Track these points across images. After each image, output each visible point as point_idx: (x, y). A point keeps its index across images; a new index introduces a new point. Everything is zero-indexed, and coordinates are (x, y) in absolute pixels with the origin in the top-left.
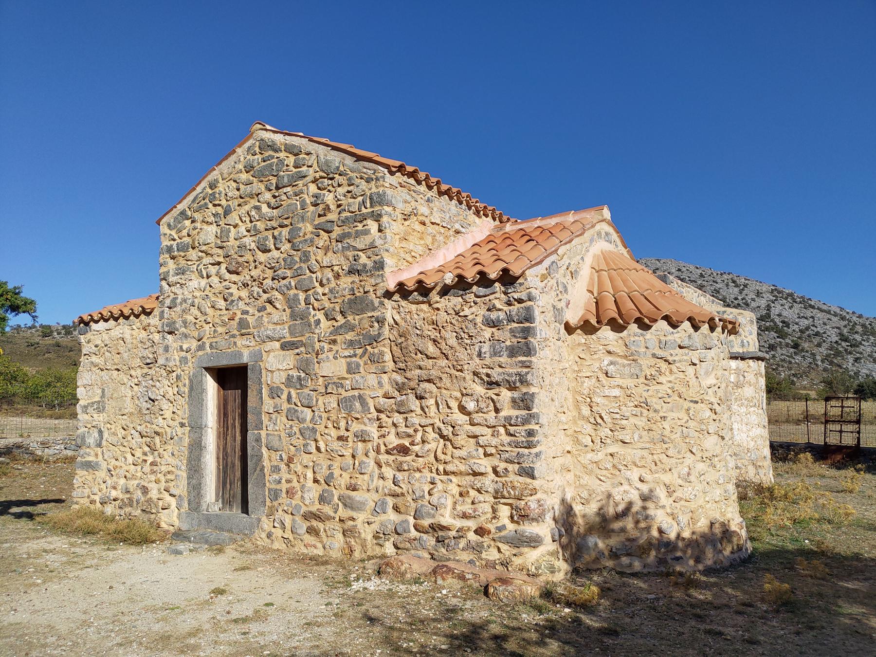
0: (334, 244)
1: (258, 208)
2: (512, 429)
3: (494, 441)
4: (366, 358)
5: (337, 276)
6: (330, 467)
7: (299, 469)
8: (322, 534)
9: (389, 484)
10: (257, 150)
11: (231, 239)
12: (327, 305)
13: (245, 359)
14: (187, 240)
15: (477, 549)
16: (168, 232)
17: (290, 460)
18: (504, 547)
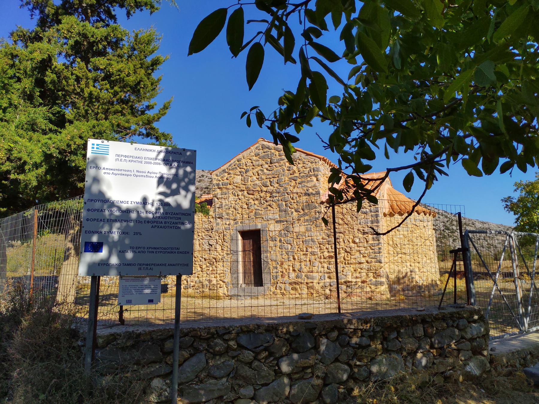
0: (298, 184)
1: (262, 171)
2: (373, 248)
3: (366, 252)
4: (314, 225)
5: (300, 196)
6: (300, 265)
7: (286, 267)
8: (299, 289)
9: (326, 269)
10: (261, 148)
11: (249, 181)
12: (296, 206)
13: (259, 226)
14: (226, 181)
15: (362, 288)
16: (217, 178)
17: (282, 264)
18: (372, 286)
